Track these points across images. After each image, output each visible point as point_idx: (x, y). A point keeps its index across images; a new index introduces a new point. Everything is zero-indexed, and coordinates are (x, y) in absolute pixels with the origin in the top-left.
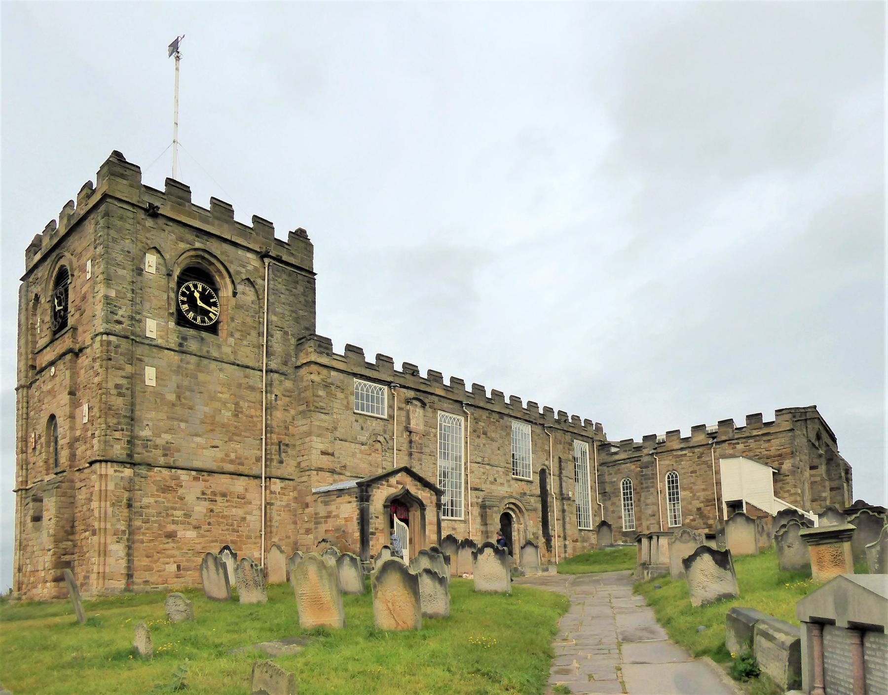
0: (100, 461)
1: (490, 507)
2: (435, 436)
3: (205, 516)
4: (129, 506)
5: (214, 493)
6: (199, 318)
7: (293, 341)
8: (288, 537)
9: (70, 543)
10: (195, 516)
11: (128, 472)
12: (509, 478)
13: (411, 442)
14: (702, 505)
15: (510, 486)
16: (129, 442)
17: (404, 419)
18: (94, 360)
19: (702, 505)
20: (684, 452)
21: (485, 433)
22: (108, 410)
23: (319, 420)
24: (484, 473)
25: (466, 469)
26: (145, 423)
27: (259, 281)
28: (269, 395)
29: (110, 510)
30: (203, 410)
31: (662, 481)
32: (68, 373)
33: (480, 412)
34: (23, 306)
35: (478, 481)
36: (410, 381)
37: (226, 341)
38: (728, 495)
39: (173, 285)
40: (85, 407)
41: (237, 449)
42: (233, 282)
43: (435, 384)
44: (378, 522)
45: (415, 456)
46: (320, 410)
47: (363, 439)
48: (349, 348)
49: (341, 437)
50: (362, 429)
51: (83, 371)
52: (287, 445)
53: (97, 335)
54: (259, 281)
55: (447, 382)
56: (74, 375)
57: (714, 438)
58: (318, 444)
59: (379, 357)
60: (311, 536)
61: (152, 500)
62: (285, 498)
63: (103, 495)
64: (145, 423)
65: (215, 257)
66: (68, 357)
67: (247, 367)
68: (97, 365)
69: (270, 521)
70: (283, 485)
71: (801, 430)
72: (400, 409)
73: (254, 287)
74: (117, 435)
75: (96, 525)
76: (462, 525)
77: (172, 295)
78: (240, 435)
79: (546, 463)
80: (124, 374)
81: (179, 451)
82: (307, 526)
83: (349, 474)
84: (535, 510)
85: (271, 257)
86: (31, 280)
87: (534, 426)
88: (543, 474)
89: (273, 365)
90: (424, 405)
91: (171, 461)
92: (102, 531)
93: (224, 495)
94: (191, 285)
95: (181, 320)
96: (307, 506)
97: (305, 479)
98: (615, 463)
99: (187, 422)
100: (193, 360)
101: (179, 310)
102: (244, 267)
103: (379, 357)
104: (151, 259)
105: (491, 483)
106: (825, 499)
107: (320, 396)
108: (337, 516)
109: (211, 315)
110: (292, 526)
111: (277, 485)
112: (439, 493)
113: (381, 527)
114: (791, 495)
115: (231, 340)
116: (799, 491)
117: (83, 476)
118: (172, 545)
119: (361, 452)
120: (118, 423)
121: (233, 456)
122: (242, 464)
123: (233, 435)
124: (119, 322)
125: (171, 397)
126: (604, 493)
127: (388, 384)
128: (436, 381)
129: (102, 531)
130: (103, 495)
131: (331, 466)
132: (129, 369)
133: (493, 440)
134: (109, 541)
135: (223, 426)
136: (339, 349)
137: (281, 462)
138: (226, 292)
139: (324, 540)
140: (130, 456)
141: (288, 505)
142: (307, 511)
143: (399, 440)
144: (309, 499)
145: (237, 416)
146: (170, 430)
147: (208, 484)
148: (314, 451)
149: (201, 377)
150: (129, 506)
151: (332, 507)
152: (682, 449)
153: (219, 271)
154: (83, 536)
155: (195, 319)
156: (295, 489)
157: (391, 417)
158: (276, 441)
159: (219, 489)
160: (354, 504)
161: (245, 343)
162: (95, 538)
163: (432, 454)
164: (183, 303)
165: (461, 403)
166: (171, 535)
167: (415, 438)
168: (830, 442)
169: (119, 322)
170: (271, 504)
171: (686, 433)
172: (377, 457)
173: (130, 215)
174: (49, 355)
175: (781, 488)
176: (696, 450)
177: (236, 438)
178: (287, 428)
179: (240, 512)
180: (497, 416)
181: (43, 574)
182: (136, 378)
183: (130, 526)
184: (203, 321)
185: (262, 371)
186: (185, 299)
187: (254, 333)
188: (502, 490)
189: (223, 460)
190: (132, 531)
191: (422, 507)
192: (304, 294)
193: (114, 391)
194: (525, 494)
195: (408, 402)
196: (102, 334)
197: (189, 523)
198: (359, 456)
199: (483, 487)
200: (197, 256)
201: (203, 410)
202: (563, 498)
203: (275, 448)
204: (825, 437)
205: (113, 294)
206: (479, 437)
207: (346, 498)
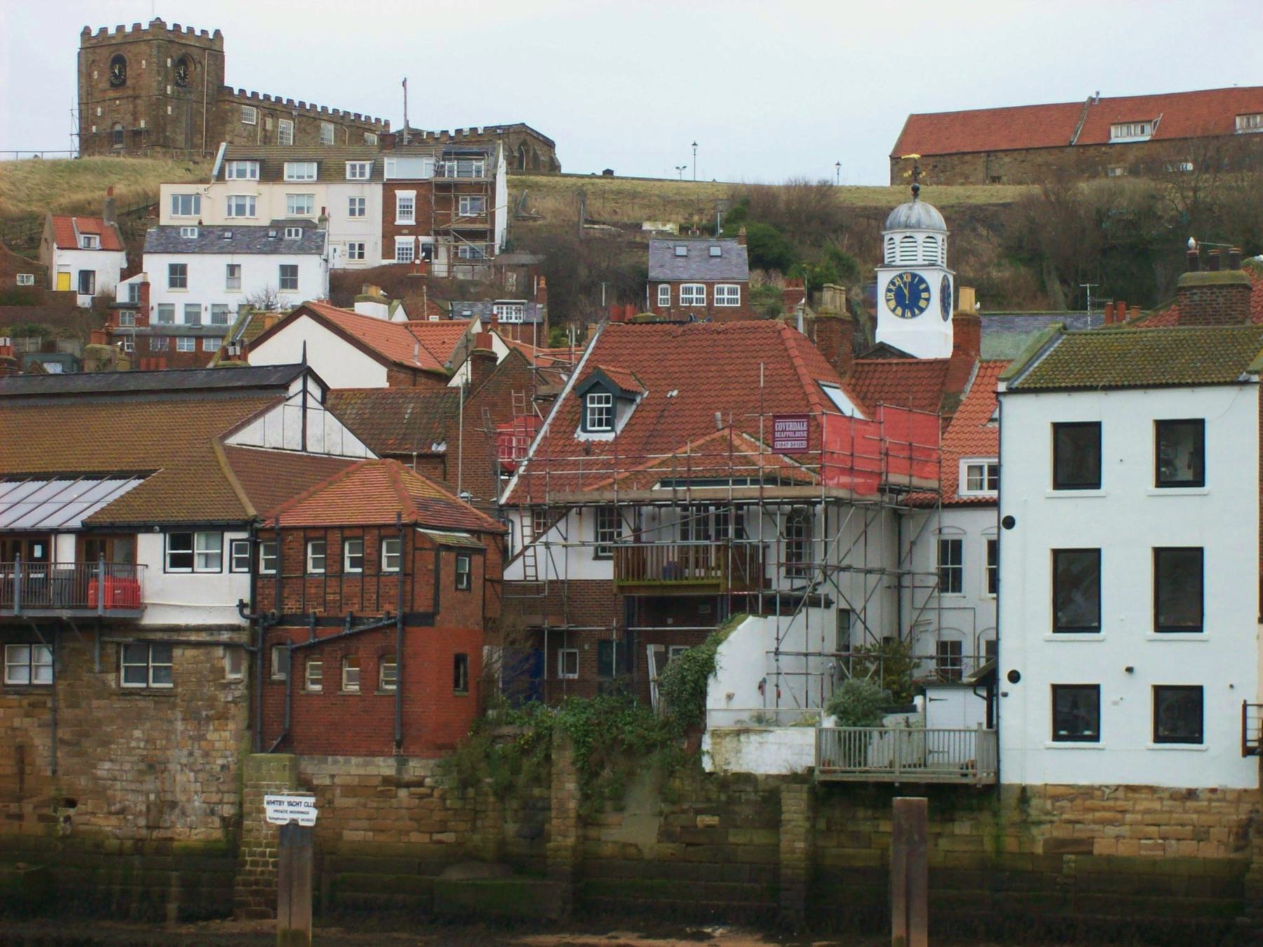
36: (266, 104)
56: (135, 107)
104: (169, 61)
136: (236, 92)
182: (166, 111)
195: (264, 115)
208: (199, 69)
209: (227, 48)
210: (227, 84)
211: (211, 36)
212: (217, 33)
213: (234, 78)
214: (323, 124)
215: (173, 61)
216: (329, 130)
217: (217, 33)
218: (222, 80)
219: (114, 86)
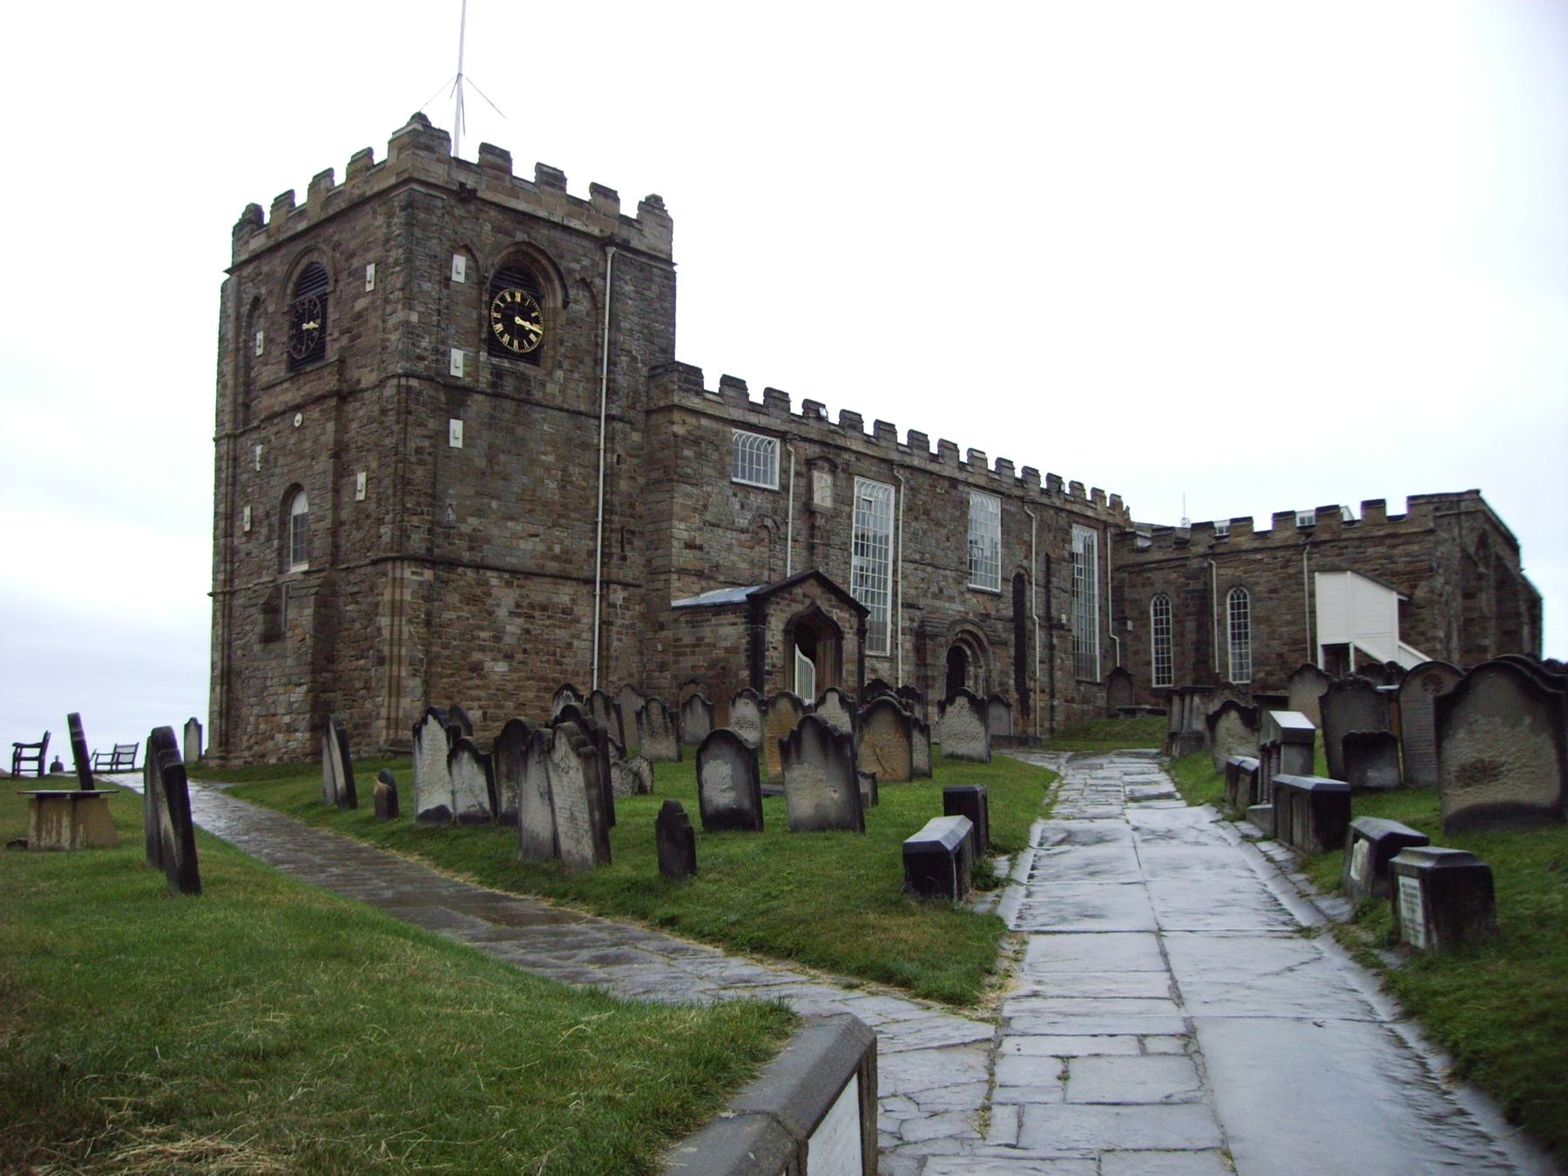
0: (394, 559)
1: (934, 636)
2: (850, 517)
5: (532, 606)
6: (516, 343)
7: (645, 371)
8: (631, 675)
9: (329, 675)
10: (508, 640)
11: (428, 574)
12: (963, 588)
13: (813, 527)
14: (1285, 649)
15: (964, 602)
16: (430, 531)
17: (802, 490)
18: (384, 412)
19: (1285, 649)
20: (1259, 556)
21: (927, 513)
22: (403, 484)
23: (683, 497)
25: (895, 572)
26: (448, 501)
27: (598, 281)
29: (406, 629)
30: (520, 481)
31: (1222, 604)
32: (330, 426)
33: (921, 479)
34: (231, 312)
35: (912, 592)
36: (813, 431)
37: (550, 374)
38: (1328, 634)
39: (485, 298)
40: (361, 478)
41: (562, 540)
42: (564, 287)
43: (850, 433)
44: (774, 656)
45: (820, 550)
46: (685, 479)
47: (743, 522)
48: (727, 381)
50: (742, 507)
51: (354, 425)
52: (633, 533)
53: (388, 378)
54: (598, 281)
55: (869, 429)
56: (342, 428)
57: (1308, 535)
58: (681, 531)
59: (769, 392)
60: (668, 674)
61: (453, 615)
62: (628, 614)
63: (397, 609)
64: (448, 501)
65: (543, 253)
66: (333, 402)
67: (580, 413)
68: (391, 419)
70: (625, 594)
71: (1449, 530)
72: (798, 474)
73: (590, 291)
74: (415, 520)
75: (386, 650)
76: (887, 665)
77: (485, 312)
78: (567, 517)
79: (1025, 563)
80: (425, 432)
81: (488, 542)
82: (659, 658)
83: (722, 578)
84: (1004, 644)
85: (617, 245)
86: (245, 273)
88: (1019, 583)
89: (615, 411)
90: (833, 468)
91: (477, 556)
92: (396, 660)
93: (544, 608)
95: (494, 345)
96: (662, 627)
97: (660, 585)
98: (1141, 568)
99: (499, 498)
100: (507, 404)
101: (491, 332)
102: (578, 261)
103: (769, 392)
104: (460, 262)
105: (935, 596)
106: (1484, 650)
107: (686, 458)
108: (714, 646)
109: (532, 337)
110: (637, 658)
111: (618, 596)
112: (862, 612)
113: (779, 663)
114: (1427, 640)
115: (559, 374)
116: (1441, 634)
117: (352, 578)
118: (477, 682)
119: (741, 544)
120: (419, 504)
121: (557, 549)
122: (570, 562)
123: (559, 515)
124: (421, 358)
125: (481, 463)
126: (1121, 620)
127: (783, 436)
129: (396, 660)
130: (397, 609)
131: (698, 565)
132: (432, 424)
133: (938, 524)
134: (404, 674)
135: (545, 504)
136: (712, 384)
138: (554, 300)
139: (693, 681)
140: (429, 550)
141: (632, 626)
142: (663, 634)
144: (664, 617)
145: (564, 487)
146: (480, 513)
147: (524, 592)
148: (675, 543)
149: (519, 430)
150: (428, 623)
151: (706, 631)
152: (1256, 550)
154: (355, 664)
155: (511, 343)
156: (642, 600)
157: (785, 487)
159: (539, 598)
160: (741, 628)
161: (576, 376)
162: (381, 669)
163: (845, 548)
164: (497, 321)
165: (890, 463)
166: (477, 668)
167: (820, 522)
168: (1505, 552)
169: (421, 358)
170: (610, 623)
171: (1263, 524)
172: (761, 552)
173: (439, 203)
174: (289, 395)
175: (1413, 628)
176: (1279, 554)
177: (563, 521)
178: (632, 506)
179: (560, 633)
181: (287, 719)
183: (427, 652)
184: (521, 346)
185: (599, 418)
186: (499, 316)
187: (588, 360)
188: (954, 608)
189: (543, 555)
190: (431, 660)
191: (839, 635)
192: (661, 297)
193: (413, 459)
194: (988, 616)
195: (810, 463)
196: (399, 376)
197: (499, 651)
198: (736, 550)
199: (922, 602)
201: (520, 481)
202: (1051, 624)
203: (616, 536)
204: (1494, 539)
205: (414, 318)
206: (916, 519)
207: (731, 618)
208: (582, 306)
209: (681, 252)
210: (683, 354)
211: (629, 209)
212: (653, 205)
213: (709, 339)
214: (976, 499)
215: (474, 267)
216: (986, 513)
217: (653, 205)
218: (669, 348)
219: (295, 367)
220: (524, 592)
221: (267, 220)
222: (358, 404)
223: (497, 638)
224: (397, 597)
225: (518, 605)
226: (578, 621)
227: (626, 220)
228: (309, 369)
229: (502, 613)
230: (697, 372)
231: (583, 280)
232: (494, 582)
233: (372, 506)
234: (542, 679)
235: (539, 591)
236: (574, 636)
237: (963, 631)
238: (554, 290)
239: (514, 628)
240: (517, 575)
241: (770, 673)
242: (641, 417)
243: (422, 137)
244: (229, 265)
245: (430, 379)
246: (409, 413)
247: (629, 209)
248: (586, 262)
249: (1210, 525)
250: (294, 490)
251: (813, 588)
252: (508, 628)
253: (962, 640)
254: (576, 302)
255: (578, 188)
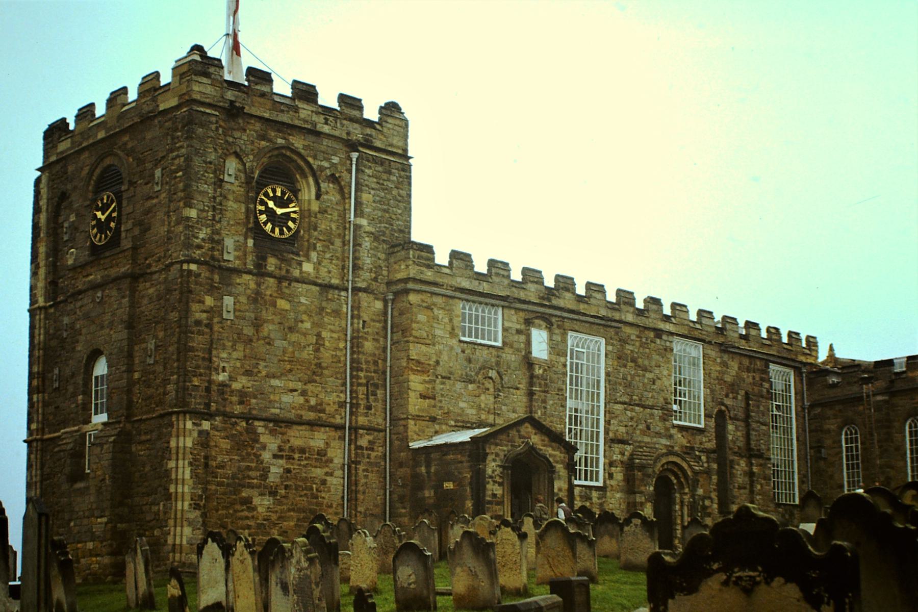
0: (178, 413)
2: (565, 366)
3: (281, 477)
4: (206, 465)
5: (292, 449)
6: (277, 230)
13: (532, 377)
18: (169, 291)
21: (634, 360)
24: (632, 419)
28: (356, 321)
36: (531, 293)
48: (455, 255)
49: (444, 374)
51: (145, 301)
54: (345, 175)
55: (581, 290)
59: (492, 263)
62: (373, 454)
69: (356, 485)
73: (339, 183)
87: (706, 345)
88: (720, 418)
93: (302, 451)
94: (270, 191)
103: (492, 263)
118: (246, 513)
122: (323, 411)
124: (199, 247)
128: (567, 290)
133: (645, 369)
136: (442, 258)
137: (369, 408)
138: (308, 192)
143: (519, 377)
146: (248, 373)
148: (412, 394)
150: (206, 465)
153: (299, 168)
155: (273, 231)
158: (363, 381)
159: (297, 443)
164: (261, 212)
167: (538, 371)
169: (199, 247)
179: (318, 472)
180: (652, 335)
184: (282, 232)
185: (346, 290)
187: (338, 242)
189: (301, 407)
191: (551, 470)
194: (692, 448)
196: (182, 262)
197: (265, 487)
200: (277, 156)
203: (362, 390)
210: (417, 236)
212: (391, 109)
217: (391, 109)
218: (406, 229)
220: (285, 437)
221: (72, 127)
222: (148, 284)
223: (264, 476)
224: (181, 444)
225: (280, 449)
226: (331, 461)
227: (369, 123)
228: (107, 254)
229: (266, 456)
230: (429, 249)
231: (333, 175)
232: (260, 430)
233: (159, 368)
234: (300, 510)
235: (298, 437)
236: (327, 474)
237: (668, 463)
238: (308, 184)
239: (276, 471)
240: (279, 423)
241: (490, 502)
242: (383, 288)
243: (199, 64)
244: (40, 164)
245: (205, 263)
246: (190, 292)
247: (371, 113)
248: (335, 160)
249: (890, 362)
250: (94, 355)
251: (527, 429)
252: (273, 469)
253: (668, 470)
254: (327, 193)
255: (328, 99)
